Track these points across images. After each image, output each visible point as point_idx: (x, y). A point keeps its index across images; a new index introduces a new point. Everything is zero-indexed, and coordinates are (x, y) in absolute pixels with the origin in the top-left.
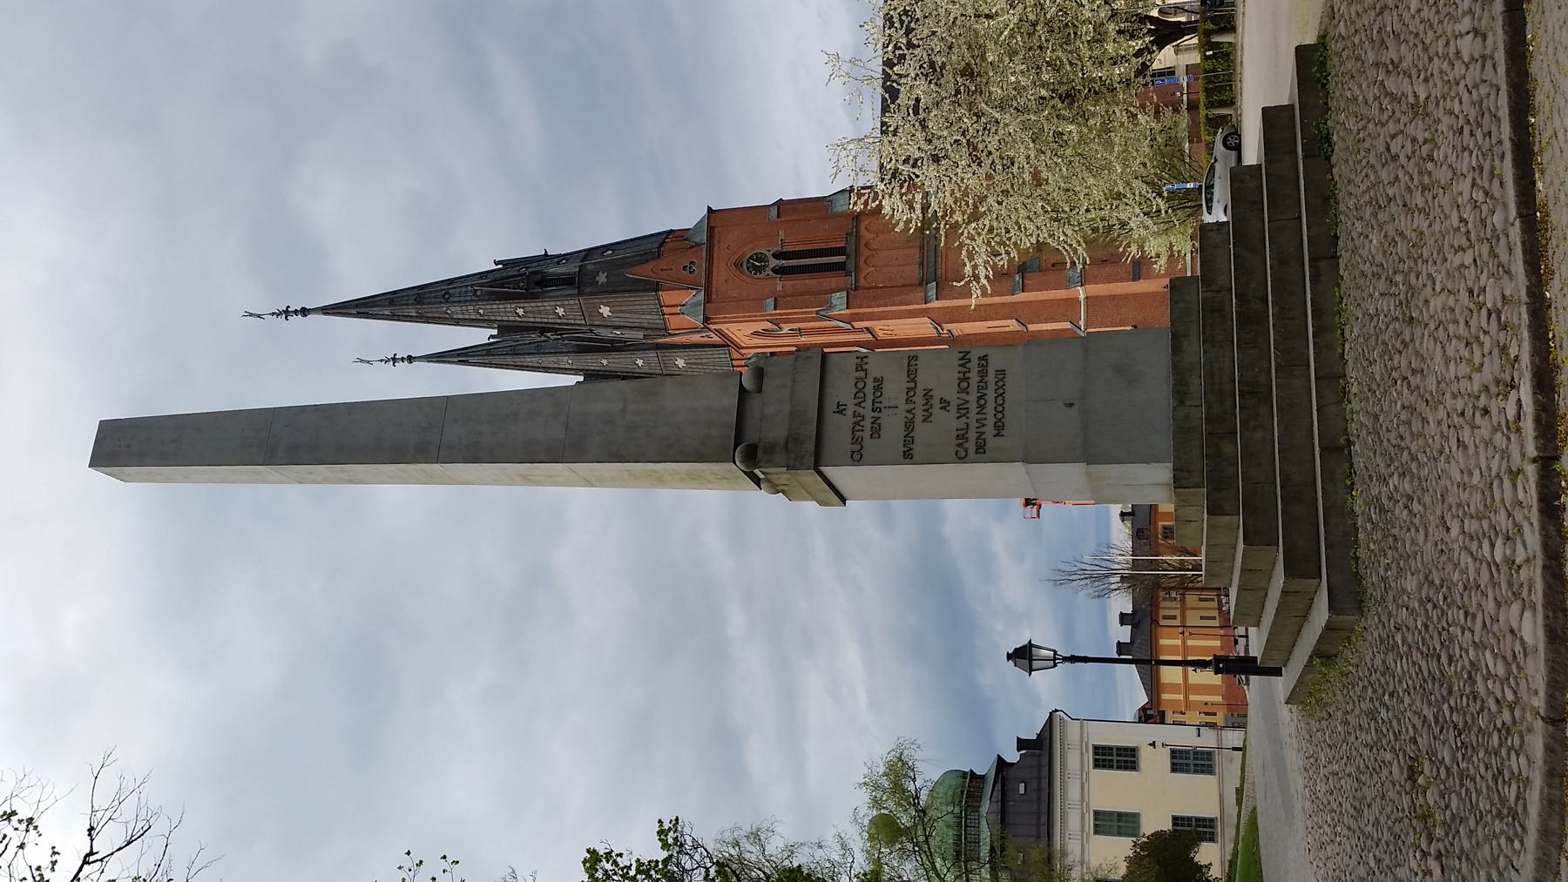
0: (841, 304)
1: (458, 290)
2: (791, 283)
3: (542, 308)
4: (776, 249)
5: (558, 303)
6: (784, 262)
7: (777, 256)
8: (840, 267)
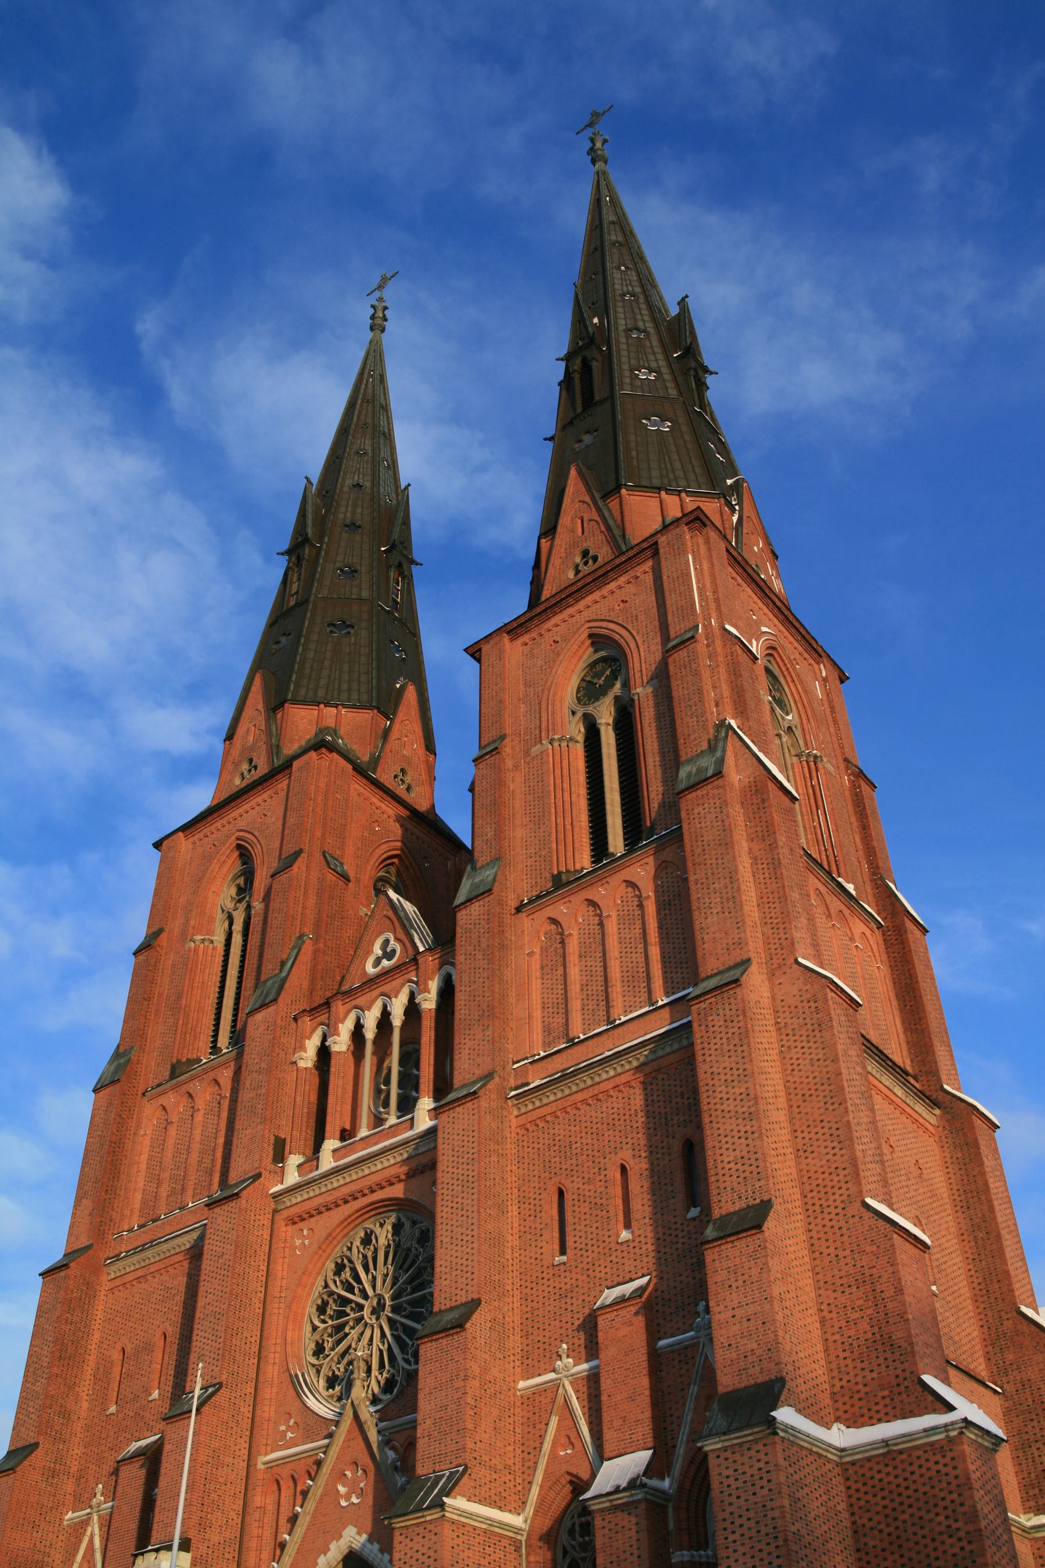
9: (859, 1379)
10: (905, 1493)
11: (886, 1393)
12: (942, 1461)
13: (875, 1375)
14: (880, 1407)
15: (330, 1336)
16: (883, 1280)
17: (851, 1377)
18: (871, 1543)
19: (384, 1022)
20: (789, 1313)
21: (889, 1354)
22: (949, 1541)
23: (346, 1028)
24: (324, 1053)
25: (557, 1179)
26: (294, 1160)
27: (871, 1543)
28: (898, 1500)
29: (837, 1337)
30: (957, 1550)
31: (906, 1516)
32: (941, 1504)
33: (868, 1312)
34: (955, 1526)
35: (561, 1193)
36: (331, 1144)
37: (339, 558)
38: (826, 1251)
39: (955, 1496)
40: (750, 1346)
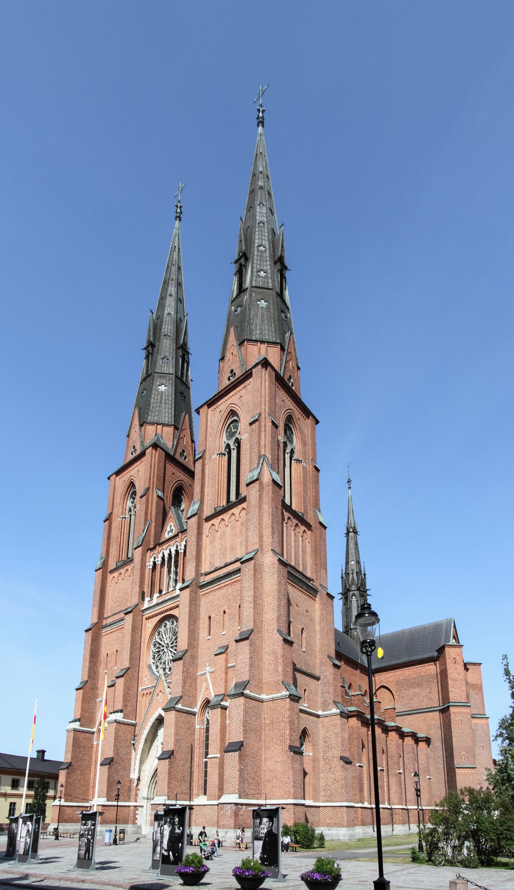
9: (270, 680)
10: (275, 710)
11: (275, 684)
12: (284, 703)
13: (273, 679)
14: (273, 688)
15: (156, 654)
16: (278, 653)
17: (268, 679)
18: (267, 722)
19: (170, 555)
20: (254, 662)
21: (277, 674)
22: (282, 723)
23: (161, 555)
25: (209, 613)
26: (147, 599)
27: (267, 722)
28: (274, 712)
29: (267, 668)
30: (283, 725)
31: (275, 716)
32: (282, 714)
33: (274, 662)
34: (284, 719)
35: (210, 617)
36: (156, 595)
37: (162, 353)
38: (267, 643)
39: (285, 712)
40: (243, 671)
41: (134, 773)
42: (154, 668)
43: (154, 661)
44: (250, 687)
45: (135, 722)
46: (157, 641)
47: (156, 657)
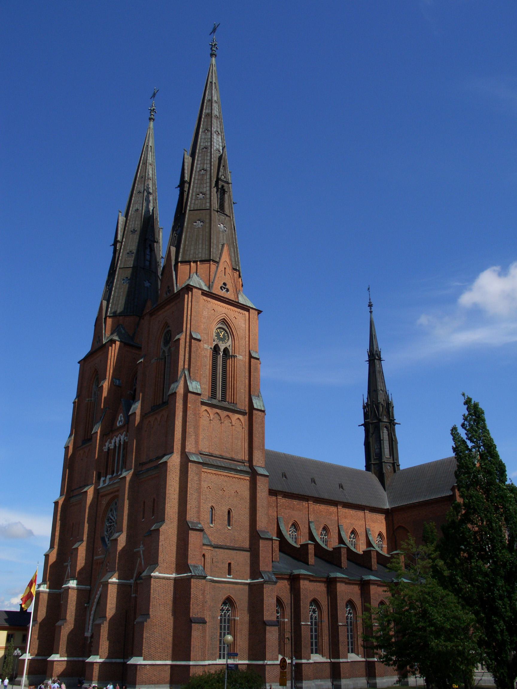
0: (193, 388)
1: (220, 141)
2: (208, 356)
3: (205, 185)
4: (230, 351)
5: (208, 196)
6: (221, 355)
7: (226, 350)
8: (213, 395)
24: (109, 449)
36: (109, 477)
41: (88, 632)
42: (107, 540)
43: (106, 534)
44: (160, 569)
45: (89, 587)
46: (109, 517)
47: (108, 530)
